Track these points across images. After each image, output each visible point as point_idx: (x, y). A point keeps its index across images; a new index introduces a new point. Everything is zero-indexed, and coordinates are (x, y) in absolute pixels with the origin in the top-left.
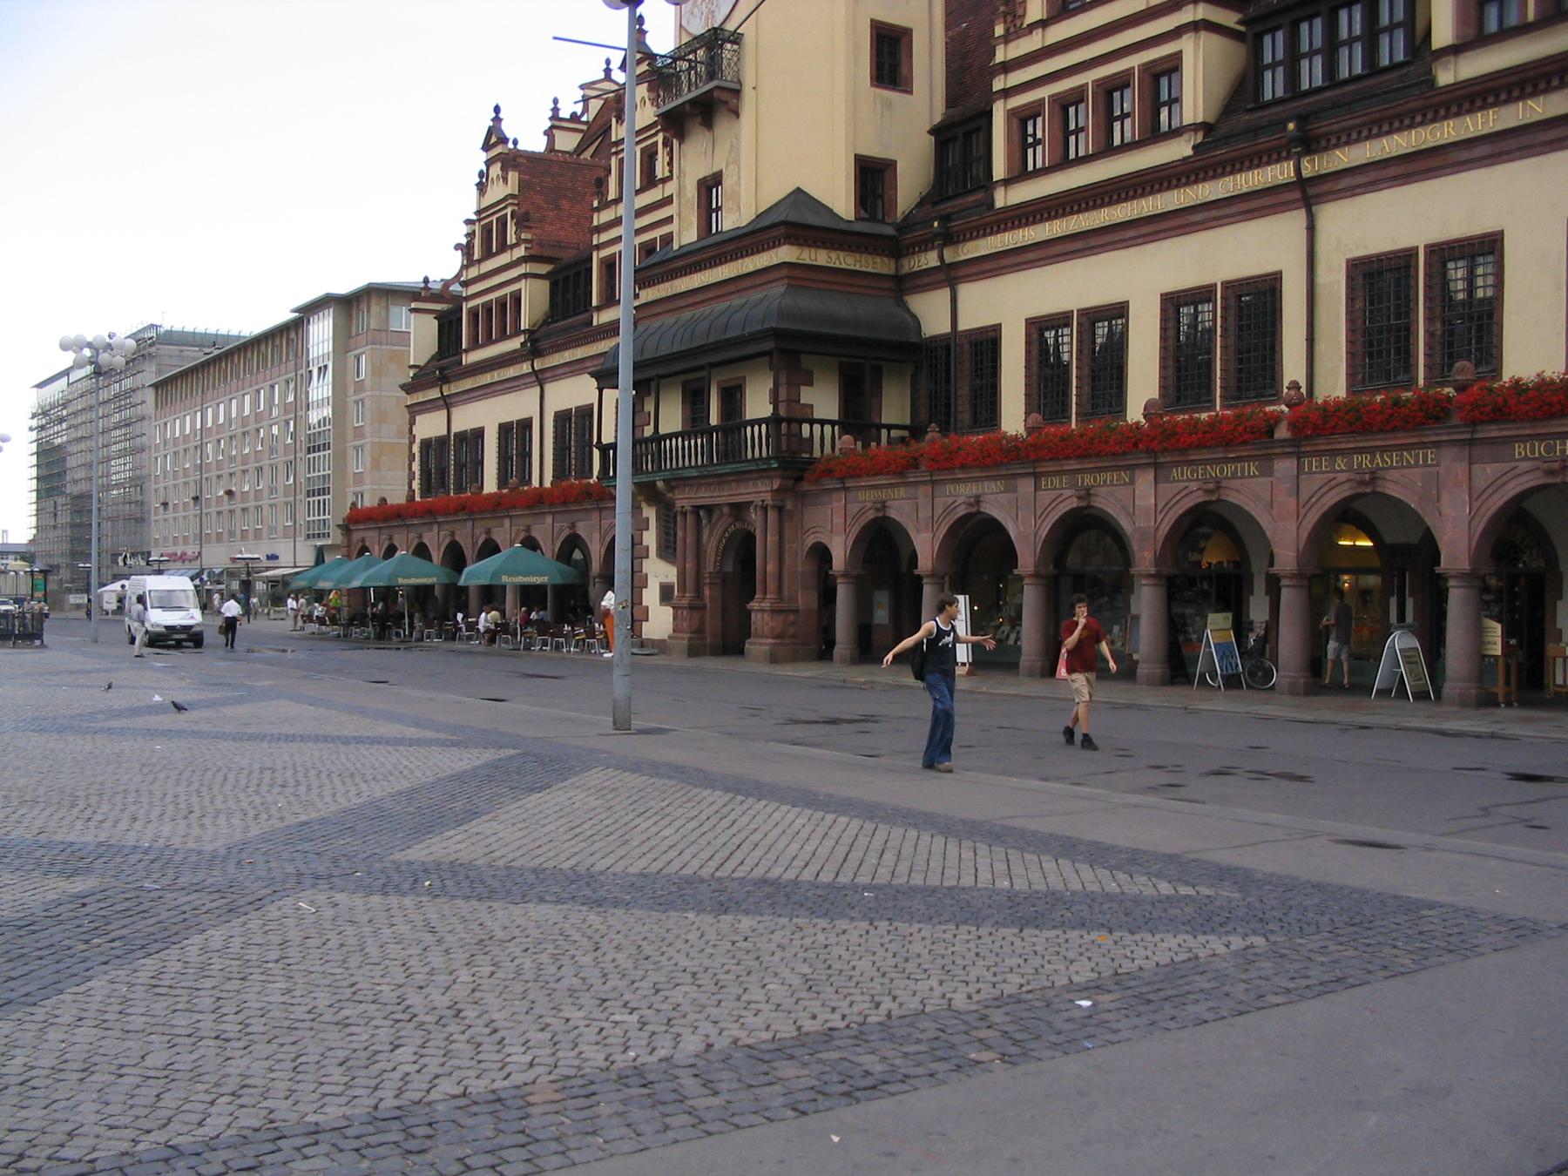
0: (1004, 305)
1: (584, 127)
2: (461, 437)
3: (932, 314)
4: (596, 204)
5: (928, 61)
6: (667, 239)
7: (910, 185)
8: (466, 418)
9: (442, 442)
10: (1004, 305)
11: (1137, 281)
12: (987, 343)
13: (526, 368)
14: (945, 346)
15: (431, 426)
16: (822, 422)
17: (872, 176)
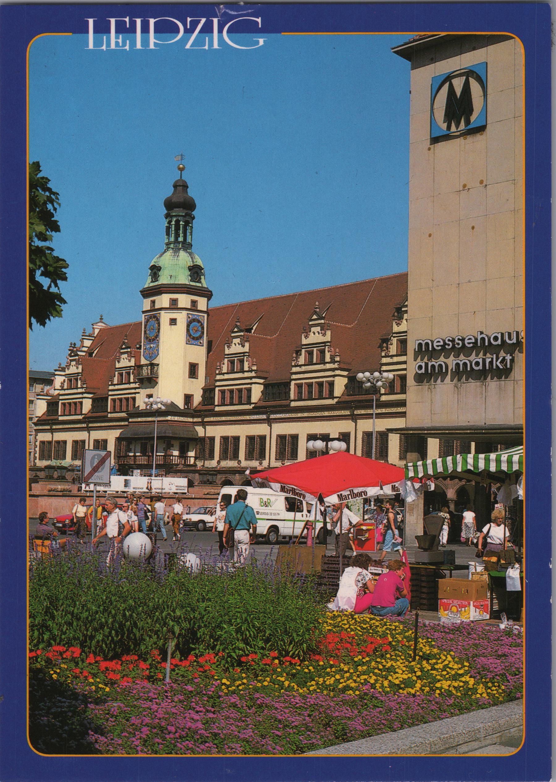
0: (217, 432)
1: (93, 338)
2: (58, 442)
3: (200, 431)
4: (110, 383)
5: (202, 371)
6: (134, 399)
7: (197, 399)
8: (59, 436)
9: (50, 443)
10: (217, 432)
11: (242, 431)
12: (212, 439)
13: (84, 425)
14: (203, 439)
15: (46, 437)
16: (175, 456)
17: (188, 398)
